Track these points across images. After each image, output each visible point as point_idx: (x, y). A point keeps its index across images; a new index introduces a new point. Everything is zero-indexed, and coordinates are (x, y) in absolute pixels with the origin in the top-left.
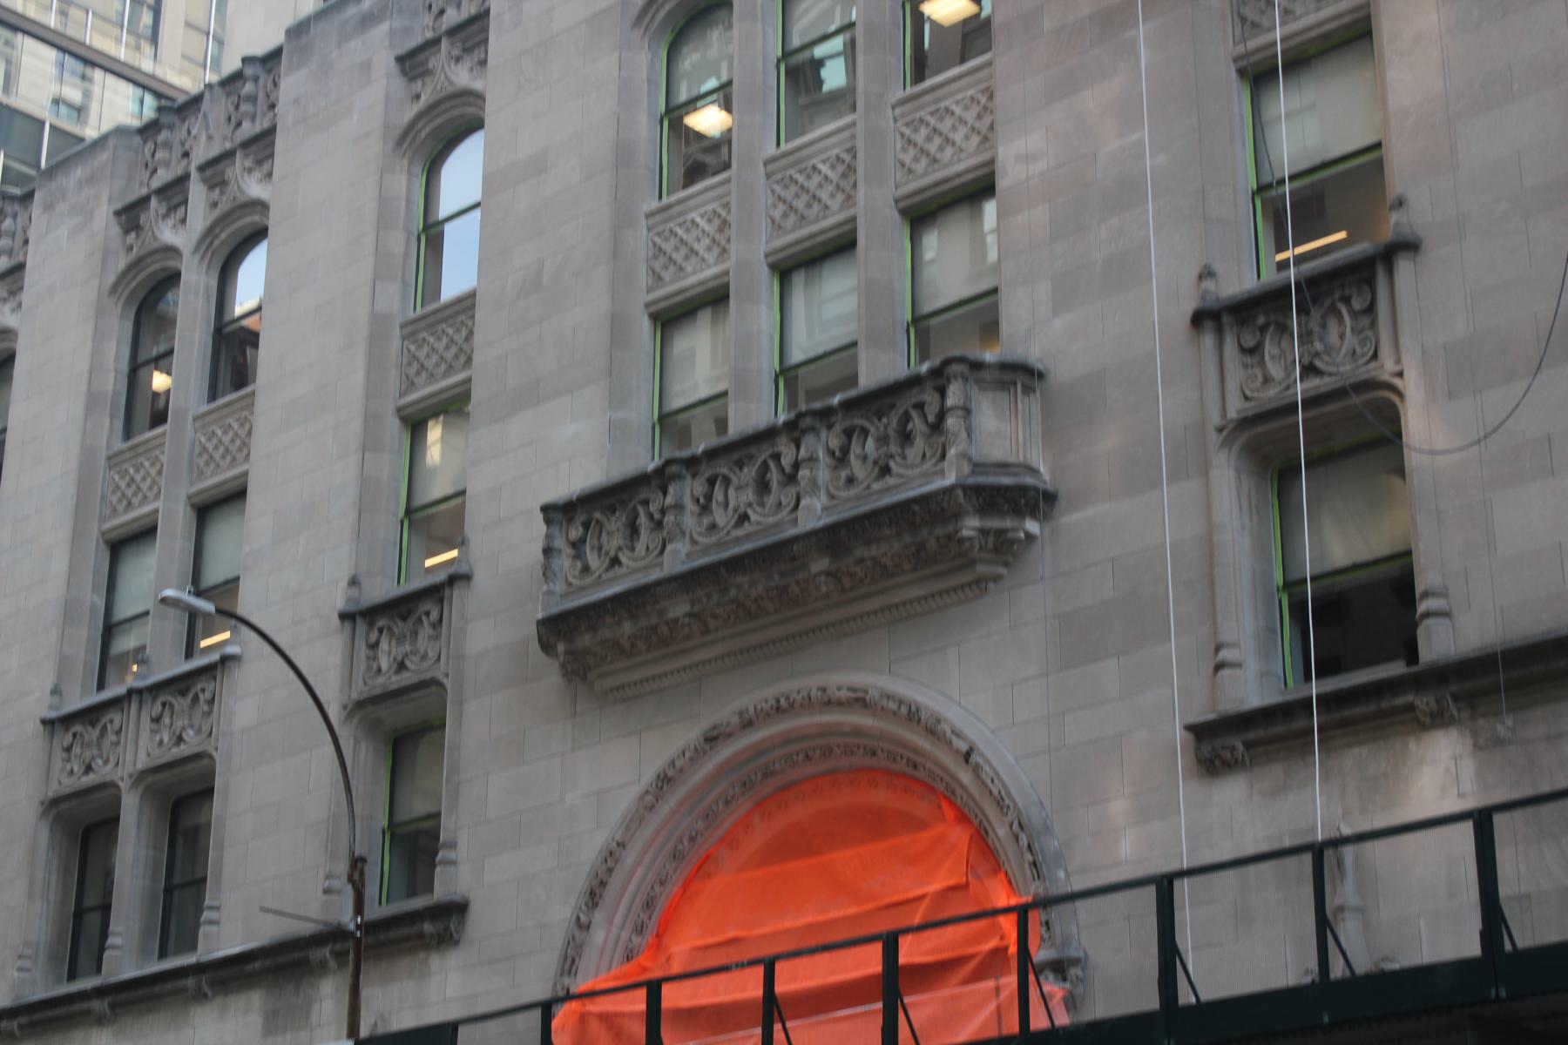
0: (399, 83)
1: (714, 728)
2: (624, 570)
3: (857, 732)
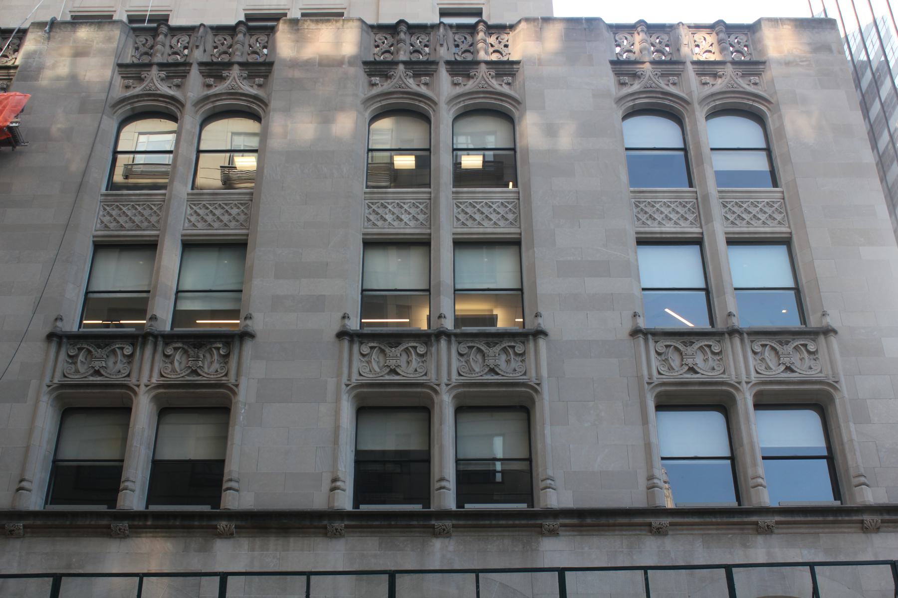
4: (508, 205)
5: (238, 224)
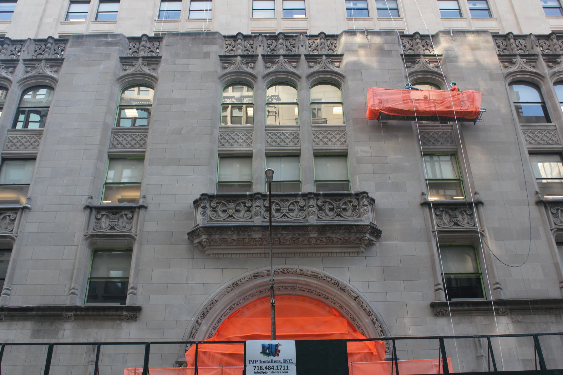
0: (119, 64)
1: (258, 273)
2: (235, 220)
3: (307, 284)
4: (277, 134)
5: (130, 145)
